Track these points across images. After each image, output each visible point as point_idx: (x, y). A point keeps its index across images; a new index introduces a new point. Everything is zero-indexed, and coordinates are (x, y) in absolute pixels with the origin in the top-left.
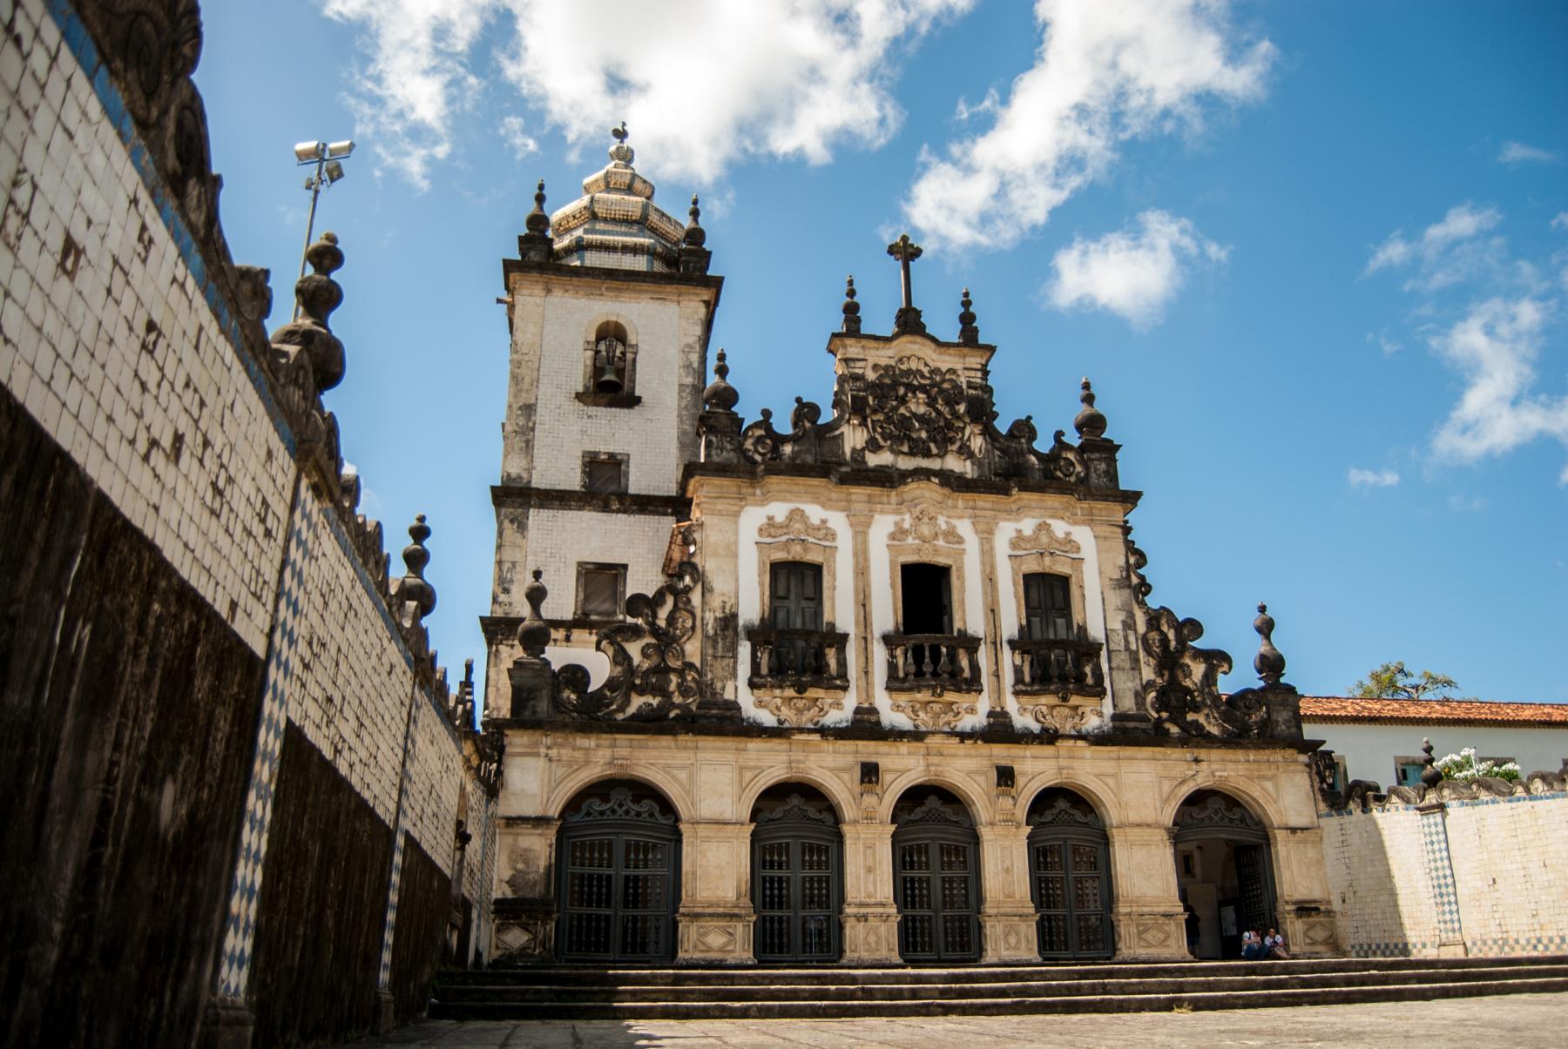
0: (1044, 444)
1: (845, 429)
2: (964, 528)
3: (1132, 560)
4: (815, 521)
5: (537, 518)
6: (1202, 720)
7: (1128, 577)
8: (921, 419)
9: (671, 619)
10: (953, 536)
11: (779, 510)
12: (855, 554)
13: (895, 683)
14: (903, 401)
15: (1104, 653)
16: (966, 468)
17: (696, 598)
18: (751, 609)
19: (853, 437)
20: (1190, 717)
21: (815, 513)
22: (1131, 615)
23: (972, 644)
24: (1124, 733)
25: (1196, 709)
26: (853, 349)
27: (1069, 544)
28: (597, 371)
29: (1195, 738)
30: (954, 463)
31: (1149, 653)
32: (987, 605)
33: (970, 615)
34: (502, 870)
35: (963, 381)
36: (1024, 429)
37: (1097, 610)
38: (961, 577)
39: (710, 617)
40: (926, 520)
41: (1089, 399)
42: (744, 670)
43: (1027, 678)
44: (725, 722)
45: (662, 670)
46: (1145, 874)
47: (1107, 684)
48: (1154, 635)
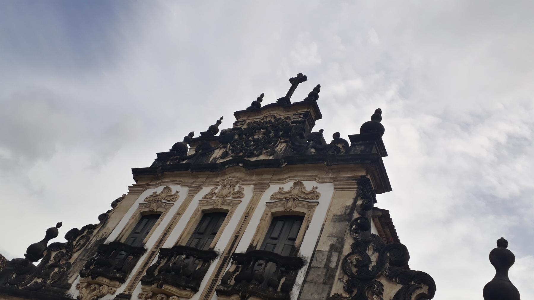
7: (351, 213)
22: (341, 241)
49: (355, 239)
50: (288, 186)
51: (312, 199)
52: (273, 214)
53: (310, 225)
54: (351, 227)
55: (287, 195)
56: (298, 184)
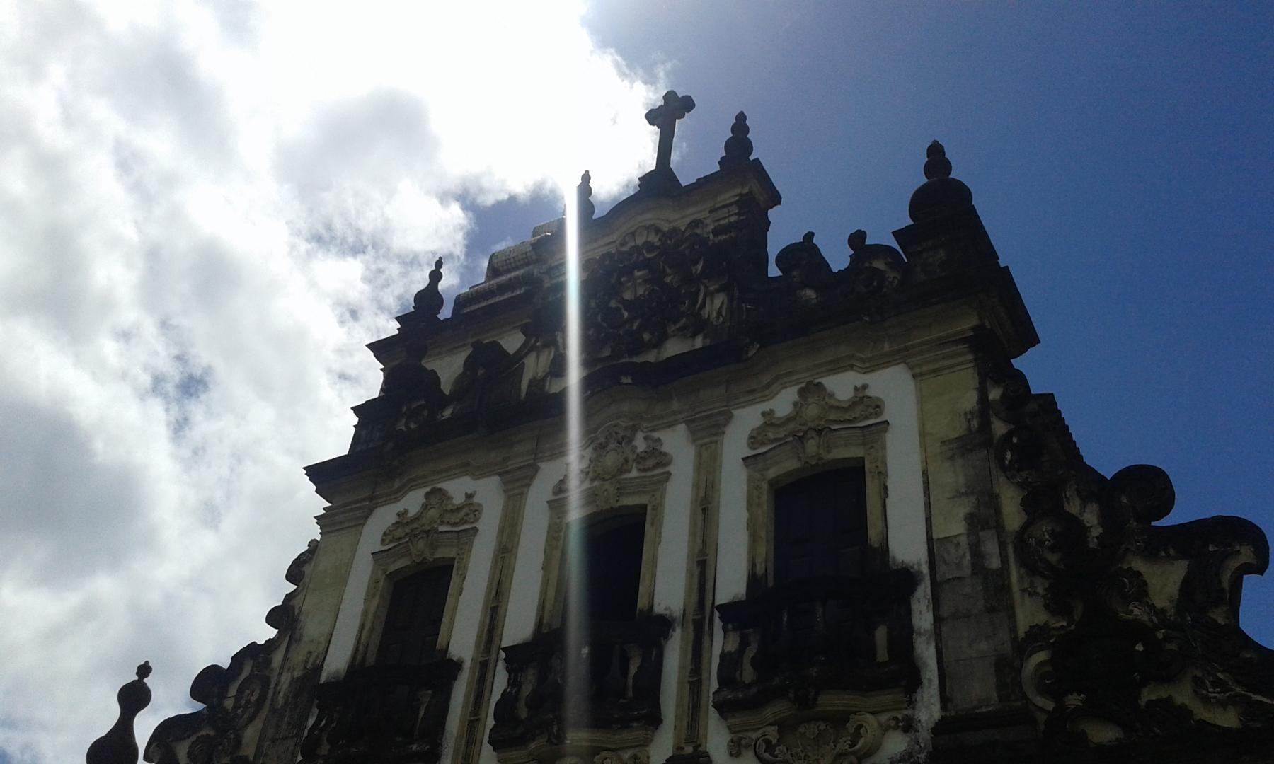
1: (530, 361)
3: (995, 394)
4: (458, 499)
6: (1183, 695)
7: (985, 425)
10: (657, 459)
12: (501, 532)
15: (923, 592)
17: (277, 658)
20: (1148, 695)
27: (865, 403)
31: (1031, 566)
38: (658, 524)
39: (286, 679)
40: (611, 446)
43: (748, 674)
47: (926, 652)
48: (1044, 529)
49: (1021, 486)
50: (783, 402)
51: (867, 418)
52: (772, 483)
53: (890, 484)
54: (1001, 459)
55: (791, 426)
56: (811, 390)
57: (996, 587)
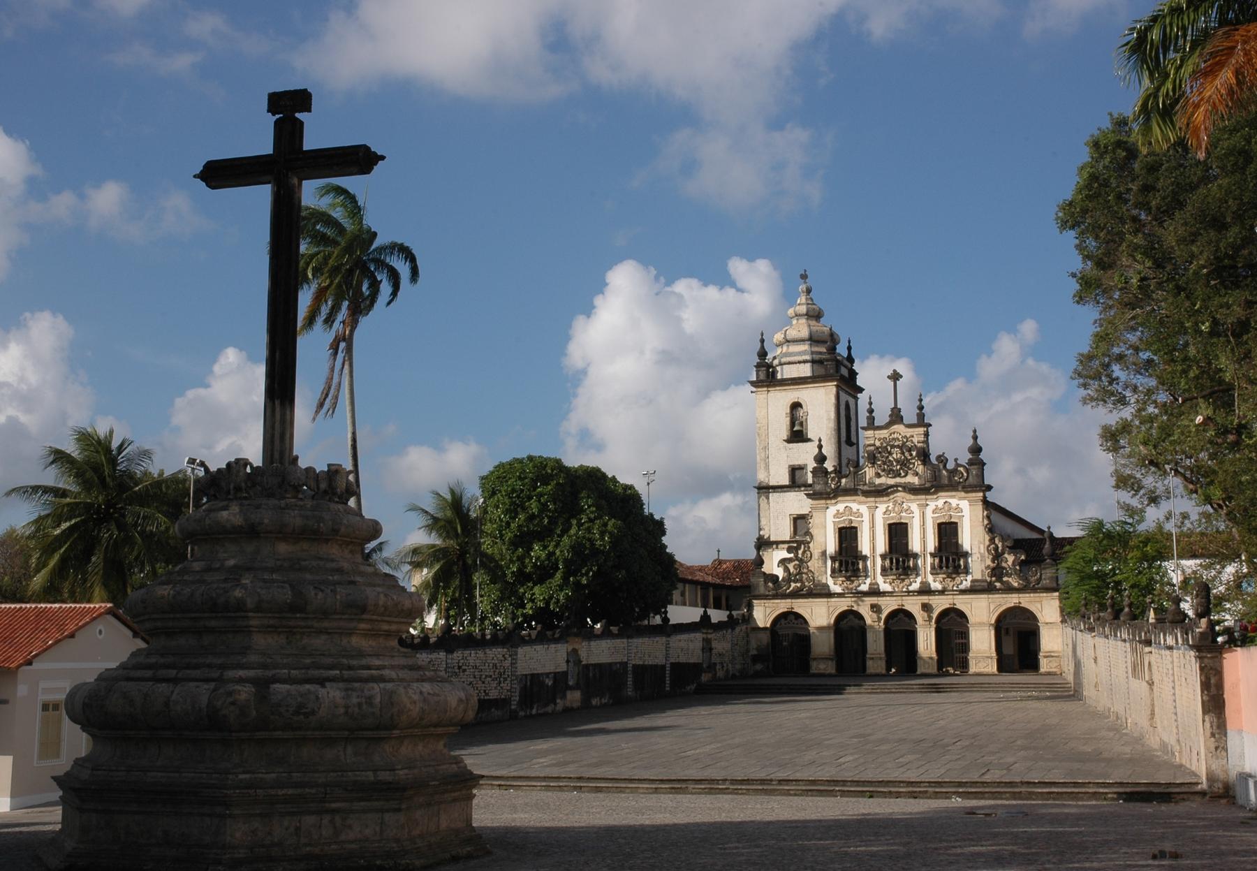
0: (951, 465)
2: (914, 507)
5: (773, 496)
8: (898, 461)
9: (804, 552)
10: (908, 510)
11: (841, 507)
13: (884, 571)
14: (890, 453)
16: (915, 480)
18: (832, 546)
19: (869, 472)
21: (855, 506)
23: (916, 556)
24: (974, 590)
25: (1009, 575)
26: (870, 433)
28: (793, 424)
29: (1009, 589)
30: (912, 479)
32: (922, 540)
33: (915, 545)
34: (753, 644)
35: (915, 440)
36: (942, 459)
37: (972, 537)
41: (975, 438)
42: (829, 572)
44: (823, 593)
45: (800, 573)
46: (982, 643)
57: (982, 556)
